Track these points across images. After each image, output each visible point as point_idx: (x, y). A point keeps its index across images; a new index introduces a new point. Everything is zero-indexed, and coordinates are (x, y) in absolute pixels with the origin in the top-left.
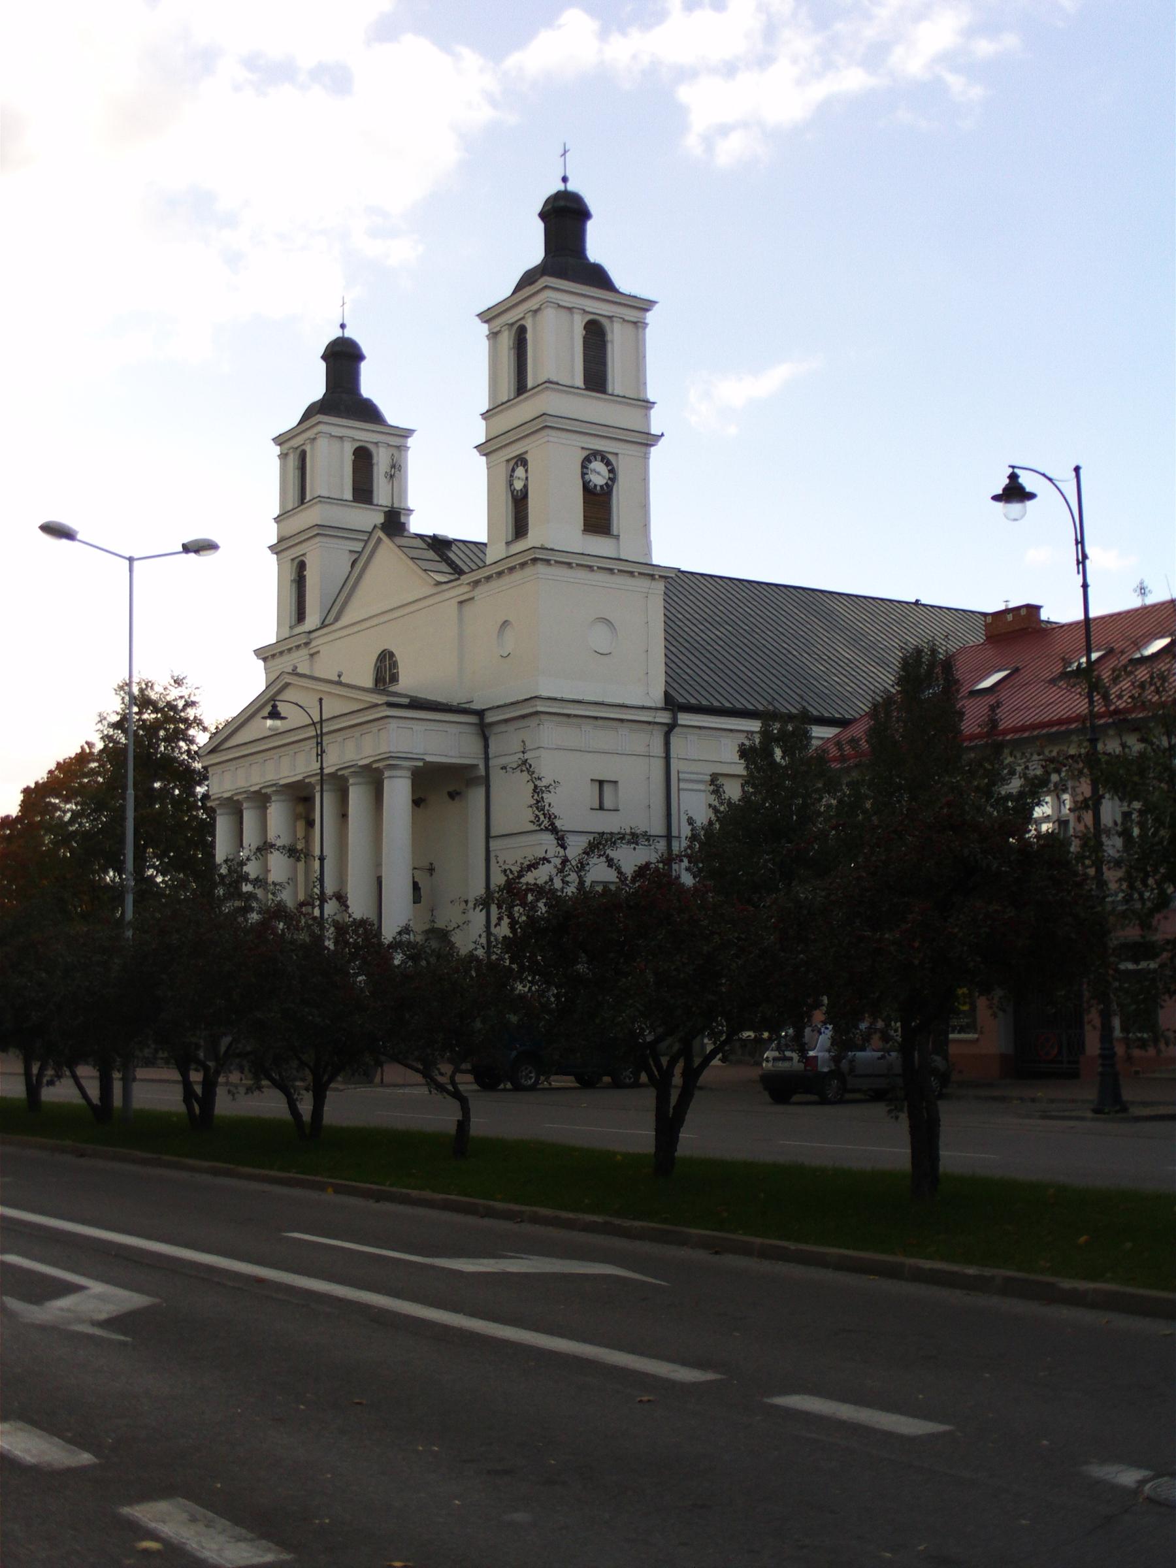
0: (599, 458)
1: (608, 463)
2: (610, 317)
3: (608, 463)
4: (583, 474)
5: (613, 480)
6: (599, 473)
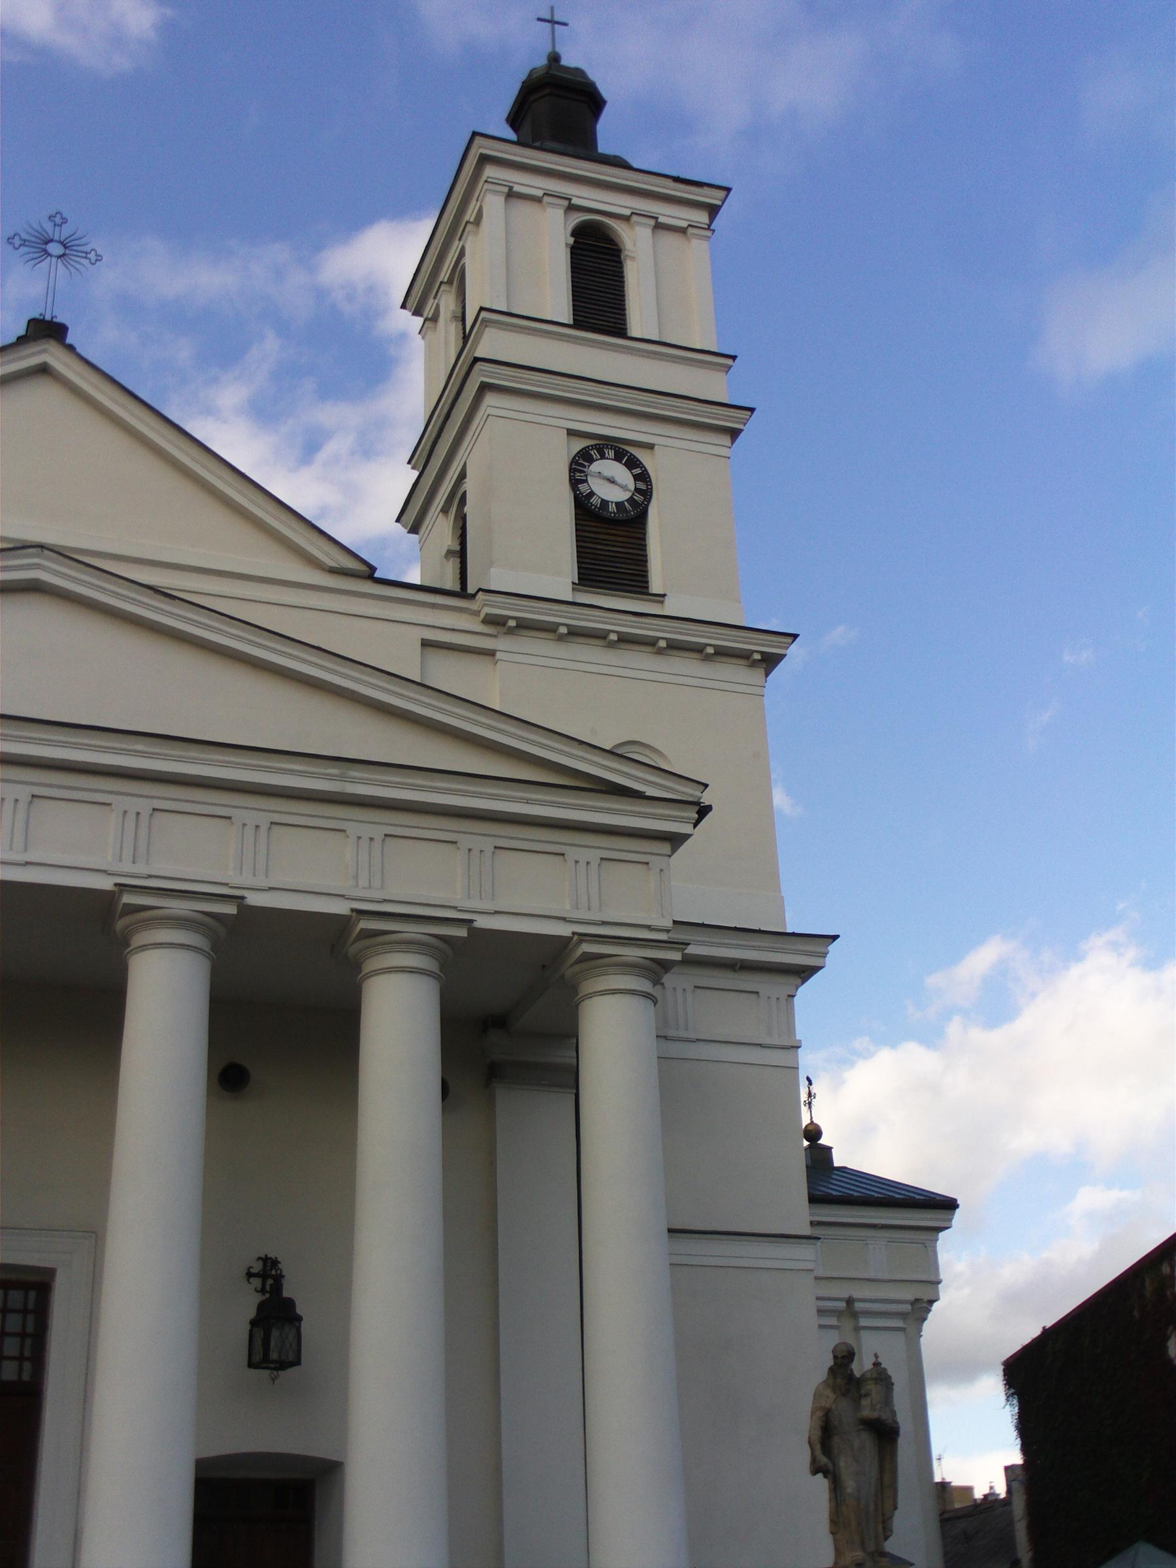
0: (612, 454)
1: (632, 463)
2: (626, 219)
3: (632, 463)
4: (575, 483)
5: (647, 494)
6: (611, 481)
